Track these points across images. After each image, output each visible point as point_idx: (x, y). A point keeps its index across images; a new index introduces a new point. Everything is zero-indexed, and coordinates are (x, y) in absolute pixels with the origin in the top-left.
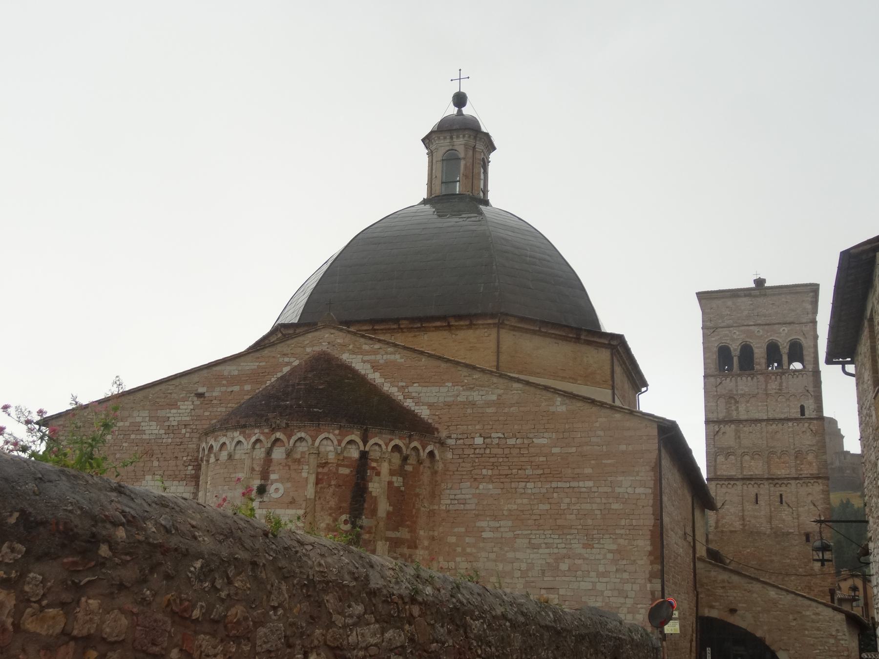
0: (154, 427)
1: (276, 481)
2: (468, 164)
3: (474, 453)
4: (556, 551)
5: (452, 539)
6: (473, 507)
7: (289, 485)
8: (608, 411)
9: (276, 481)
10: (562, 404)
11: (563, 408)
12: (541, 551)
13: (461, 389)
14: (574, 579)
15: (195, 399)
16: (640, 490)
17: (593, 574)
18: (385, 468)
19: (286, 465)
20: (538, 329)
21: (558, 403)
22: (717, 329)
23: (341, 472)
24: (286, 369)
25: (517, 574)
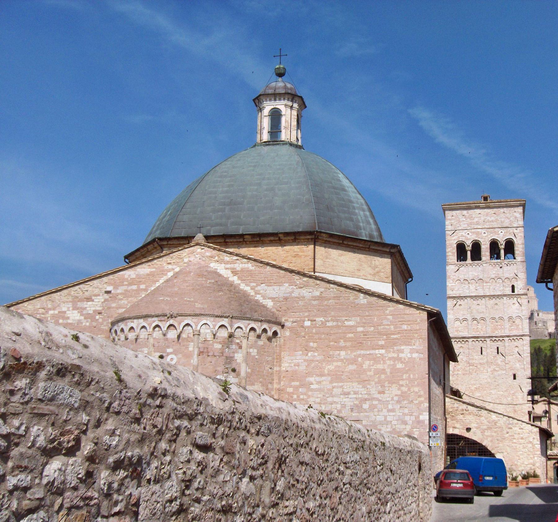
0: (76, 315)
1: (171, 353)
4: (360, 396)
5: (290, 390)
7: (180, 356)
8: (394, 304)
9: (171, 353)
11: (365, 301)
12: (350, 396)
13: (295, 288)
16: (415, 355)
21: (361, 298)
22: (456, 231)
23: (216, 347)
24: (170, 274)
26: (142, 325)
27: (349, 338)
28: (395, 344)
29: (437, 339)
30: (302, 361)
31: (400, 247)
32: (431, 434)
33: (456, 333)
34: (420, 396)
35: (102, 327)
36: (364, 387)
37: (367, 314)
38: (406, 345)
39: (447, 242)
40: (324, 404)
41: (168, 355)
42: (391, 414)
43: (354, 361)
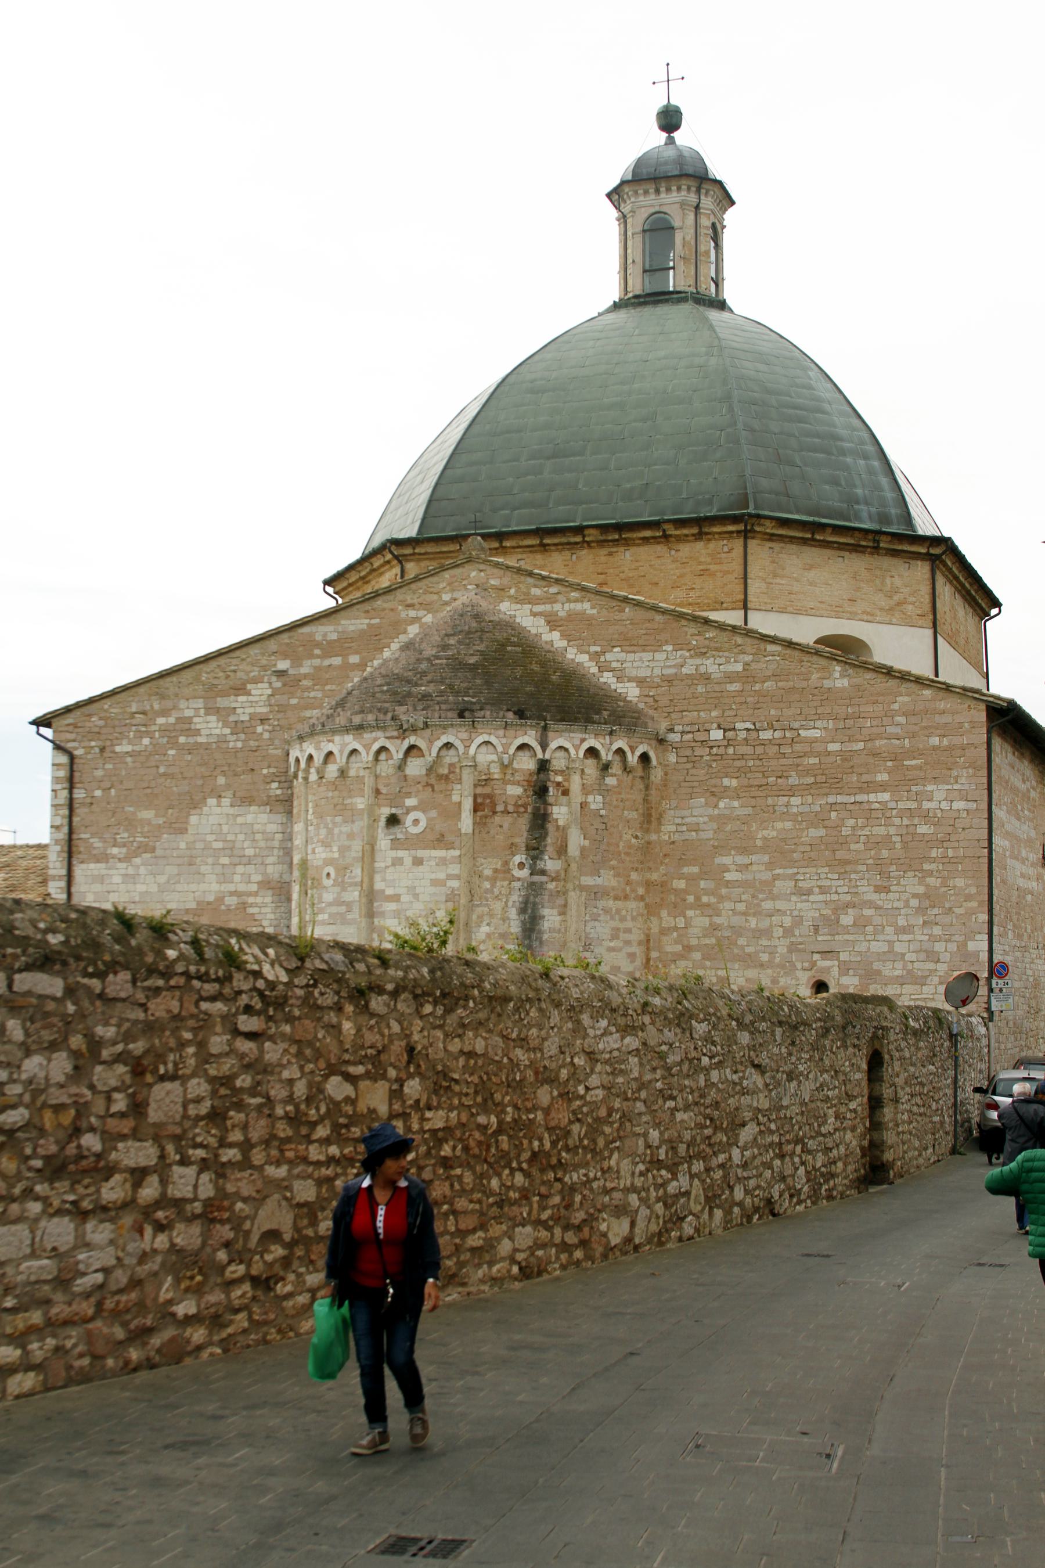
0: (214, 725)
1: (414, 808)
2: (688, 238)
3: (710, 754)
4: (835, 897)
5: (681, 884)
6: (710, 834)
7: (433, 814)
9: (414, 808)
10: (842, 676)
11: (845, 682)
12: (812, 898)
13: (688, 654)
14: (862, 938)
15: (274, 679)
17: (889, 930)
18: (575, 783)
19: (428, 784)
24: (413, 630)
25: (778, 932)
26: (350, 748)
28: (914, 781)
29: (1031, 761)
30: (706, 819)
32: (994, 982)
34: (969, 898)
35: (270, 751)
36: (842, 875)
40: (754, 914)
41: (407, 813)
43: (819, 819)
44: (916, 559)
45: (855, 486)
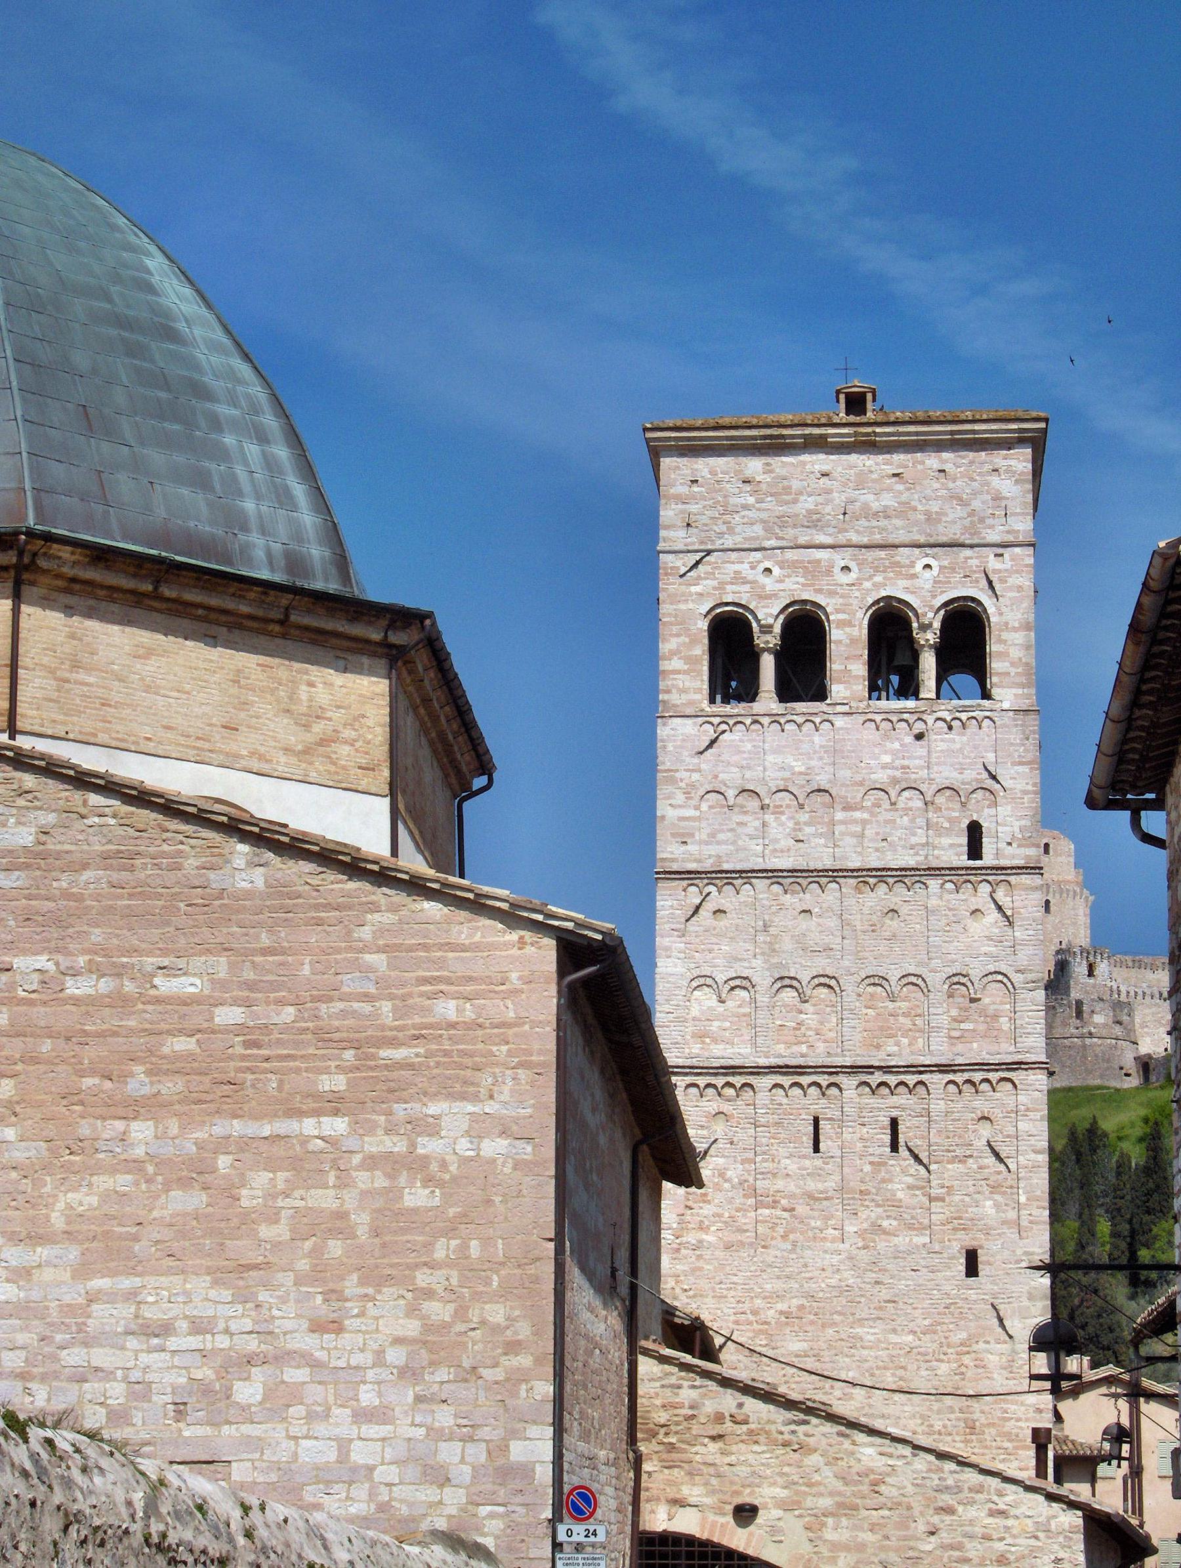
4: (223, 1342)
8: (399, 897)
11: (257, 879)
12: (173, 1343)
16: (495, 1147)
20: (150, 588)
22: (709, 552)
27: (177, 1057)
28: (395, 1092)
29: (602, 1072)
31: (434, 624)
32: (562, 1529)
33: (696, 1049)
34: (513, 1347)
36: (243, 1297)
37: (265, 940)
38: (452, 1096)
39: (666, 608)
40: (44, 1378)
42: (374, 1430)
44: (361, 652)
45: (240, 494)
